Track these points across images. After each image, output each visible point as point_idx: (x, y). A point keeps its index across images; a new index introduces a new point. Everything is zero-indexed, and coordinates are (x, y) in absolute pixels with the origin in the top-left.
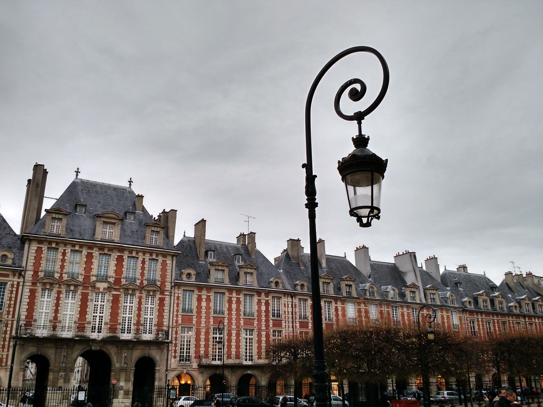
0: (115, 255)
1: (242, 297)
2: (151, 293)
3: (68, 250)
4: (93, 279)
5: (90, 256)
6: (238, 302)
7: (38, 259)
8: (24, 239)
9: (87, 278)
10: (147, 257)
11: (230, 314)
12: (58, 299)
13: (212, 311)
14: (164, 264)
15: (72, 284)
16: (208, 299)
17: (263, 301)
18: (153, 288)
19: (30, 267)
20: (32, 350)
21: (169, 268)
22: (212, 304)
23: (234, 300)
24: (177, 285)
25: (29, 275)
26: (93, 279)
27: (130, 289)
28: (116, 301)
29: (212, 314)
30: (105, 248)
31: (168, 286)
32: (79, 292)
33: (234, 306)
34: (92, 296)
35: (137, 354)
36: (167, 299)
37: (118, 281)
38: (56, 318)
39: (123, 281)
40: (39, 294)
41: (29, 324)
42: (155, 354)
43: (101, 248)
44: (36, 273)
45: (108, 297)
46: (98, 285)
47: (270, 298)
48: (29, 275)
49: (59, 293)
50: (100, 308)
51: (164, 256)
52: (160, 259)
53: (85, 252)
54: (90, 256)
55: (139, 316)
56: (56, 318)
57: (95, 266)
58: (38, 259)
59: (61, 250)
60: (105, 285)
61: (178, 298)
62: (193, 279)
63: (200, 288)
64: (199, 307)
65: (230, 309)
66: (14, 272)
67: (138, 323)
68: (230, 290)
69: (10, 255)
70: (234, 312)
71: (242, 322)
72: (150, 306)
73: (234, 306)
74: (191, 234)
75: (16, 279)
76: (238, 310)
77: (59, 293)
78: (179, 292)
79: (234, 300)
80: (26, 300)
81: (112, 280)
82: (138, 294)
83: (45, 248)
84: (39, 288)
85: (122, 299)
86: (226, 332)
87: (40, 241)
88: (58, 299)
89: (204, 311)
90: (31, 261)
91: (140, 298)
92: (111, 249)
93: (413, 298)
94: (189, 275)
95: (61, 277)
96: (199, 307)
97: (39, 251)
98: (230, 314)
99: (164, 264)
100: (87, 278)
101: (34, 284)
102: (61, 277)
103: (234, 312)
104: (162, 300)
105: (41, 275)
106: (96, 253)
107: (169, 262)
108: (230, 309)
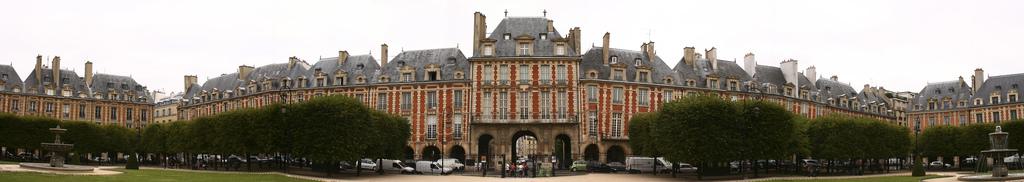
0: (532, 65)
1: (637, 91)
2: (562, 90)
3: (498, 66)
4: (517, 83)
5: (513, 68)
6: (634, 94)
7: (479, 73)
8: (471, 61)
9: (513, 83)
10: (556, 64)
11: (627, 103)
12: (495, 98)
13: (612, 101)
14: (570, 68)
15: (503, 88)
16: (609, 92)
17: (656, 95)
18: (564, 87)
19: (475, 79)
20: (482, 131)
21: (574, 70)
22: (612, 96)
23: (631, 93)
24: (581, 83)
25: (475, 84)
26: (517, 83)
27: (545, 89)
28: (535, 97)
29: (612, 103)
30: (524, 61)
31: (575, 84)
32: (509, 92)
33: (631, 97)
34: (518, 95)
35: (555, 132)
36: (575, 94)
37: (535, 83)
38: (495, 110)
39: (540, 83)
40: (482, 96)
41: (478, 115)
42: (569, 132)
43: (521, 61)
44: (479, 83)
45: (530, 95)
46: (521, 87)
47: (662, 91)
48: (475, 84)
49: (495, 94)
50: (525, 103)
51: (570, 62)
52: (567, 65)
53: (509, 65)
54: (513, 68)
55: (554, 106)
56: (495, 110)
57: (517, 74)
58: (479, 73)
59: (493, 66)
60: (527, 87)
61: (584, 92)
62: (596, 78)
63: (602, 84)
64: (601, 98)
65: (627, 100)
66: (465, 83)
67: (554, 111)
68: (627, 86)
69: (462, 73)
70: (630, 102)
71: (637, 109)
72: (562, 100)
73: (631, 97)
74: (600, 44)
75: (467, 88)
76: (634, 100)
77: (495, 94)
78: (585, 88)
79: (631, 93)
80: (475, 100)
81: (531, 83)
82: (551, 91)
83: (482, 66)
84: (482, 92)
85: (540, 95)
86: (623, 117)
87: (479, 62)
88: (495, 98)
89: (605, 100)
90: (475, 75)
91: (554, 94)
92: (528, 61)
93: (789, 94)
94: (593, 74)
95: (495, 84)
96: (601, 98)
97: (479, 68)
98: (627, 103)
99: (570, 68)
100: (513, 83)
101: (479, 90)
102: (495, 84)
103: (630, 102)
104: (571, 95)
105: (482, 83)
106: (517, 65)
107: (574, 66)
108: (627, 100)
